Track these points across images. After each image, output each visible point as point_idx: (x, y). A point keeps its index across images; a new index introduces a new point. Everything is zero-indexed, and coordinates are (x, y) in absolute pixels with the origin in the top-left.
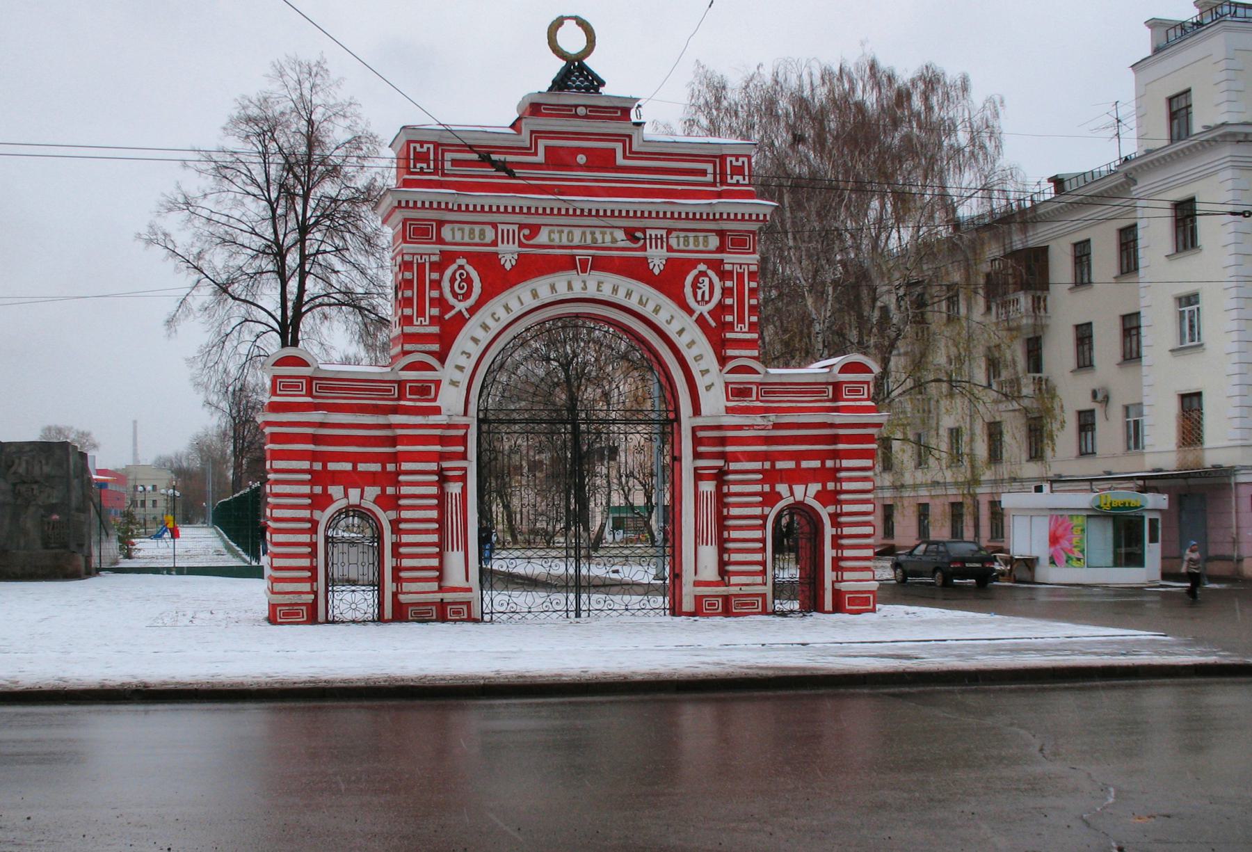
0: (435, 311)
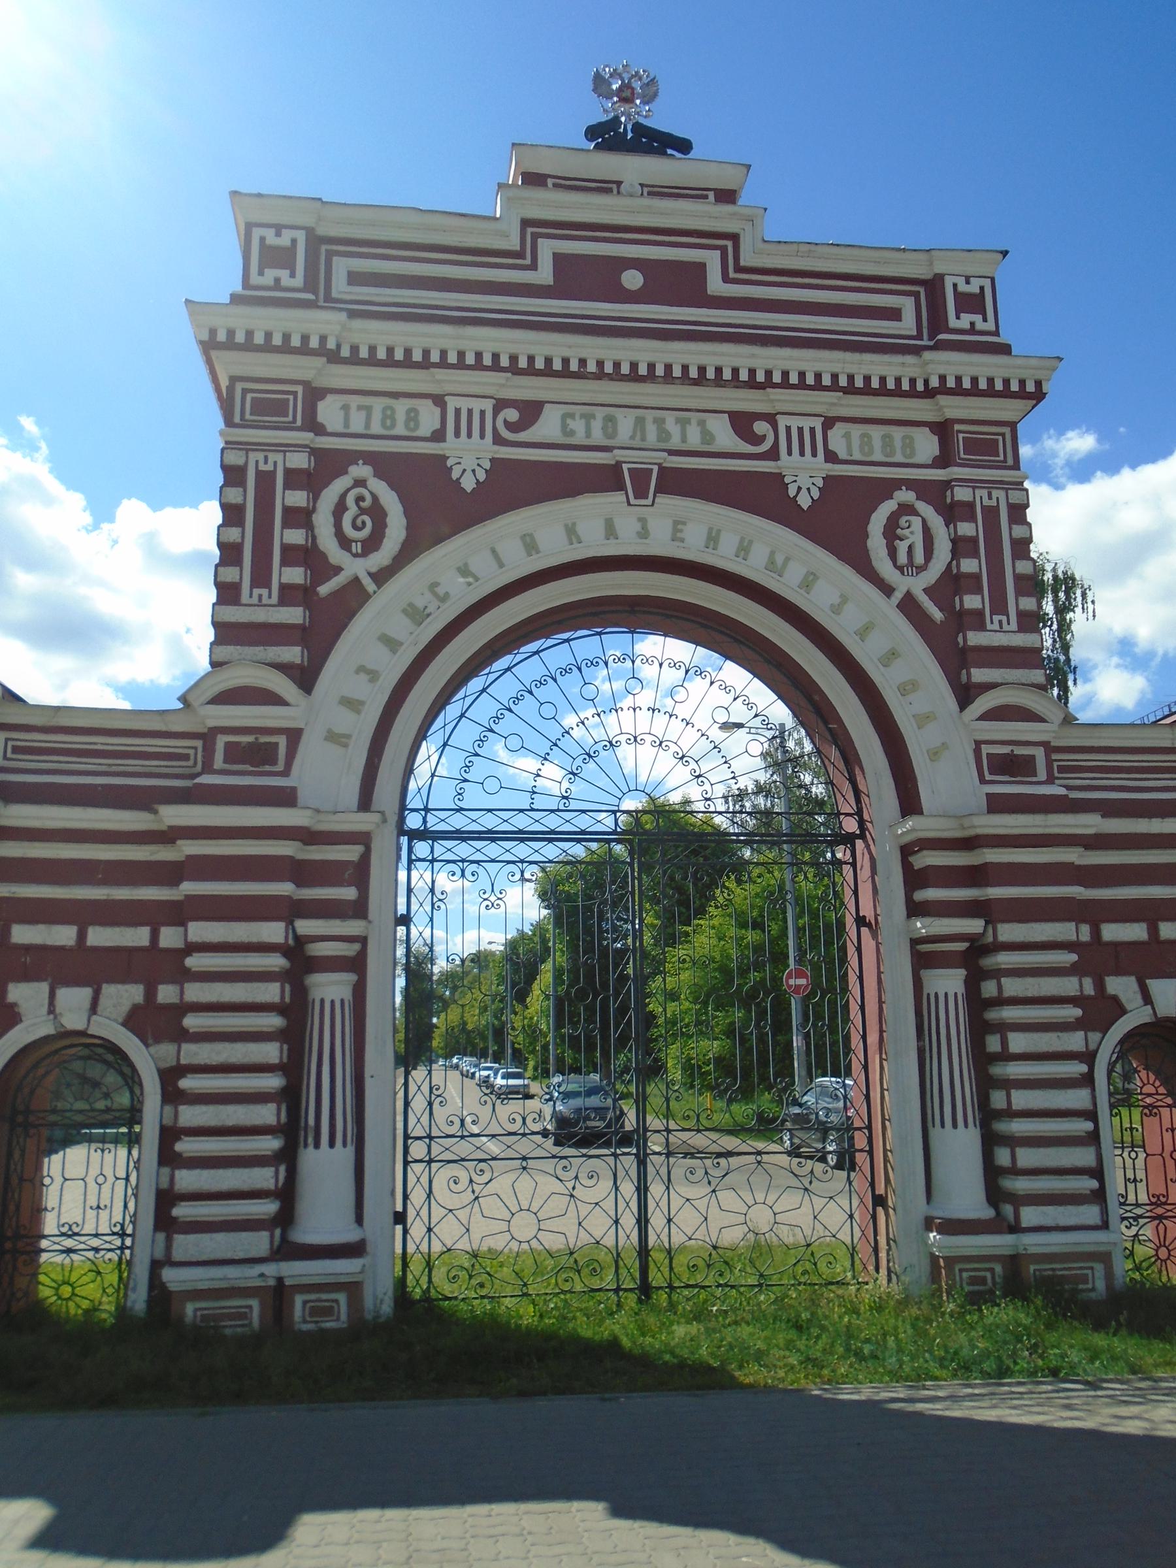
0: (295, 575)
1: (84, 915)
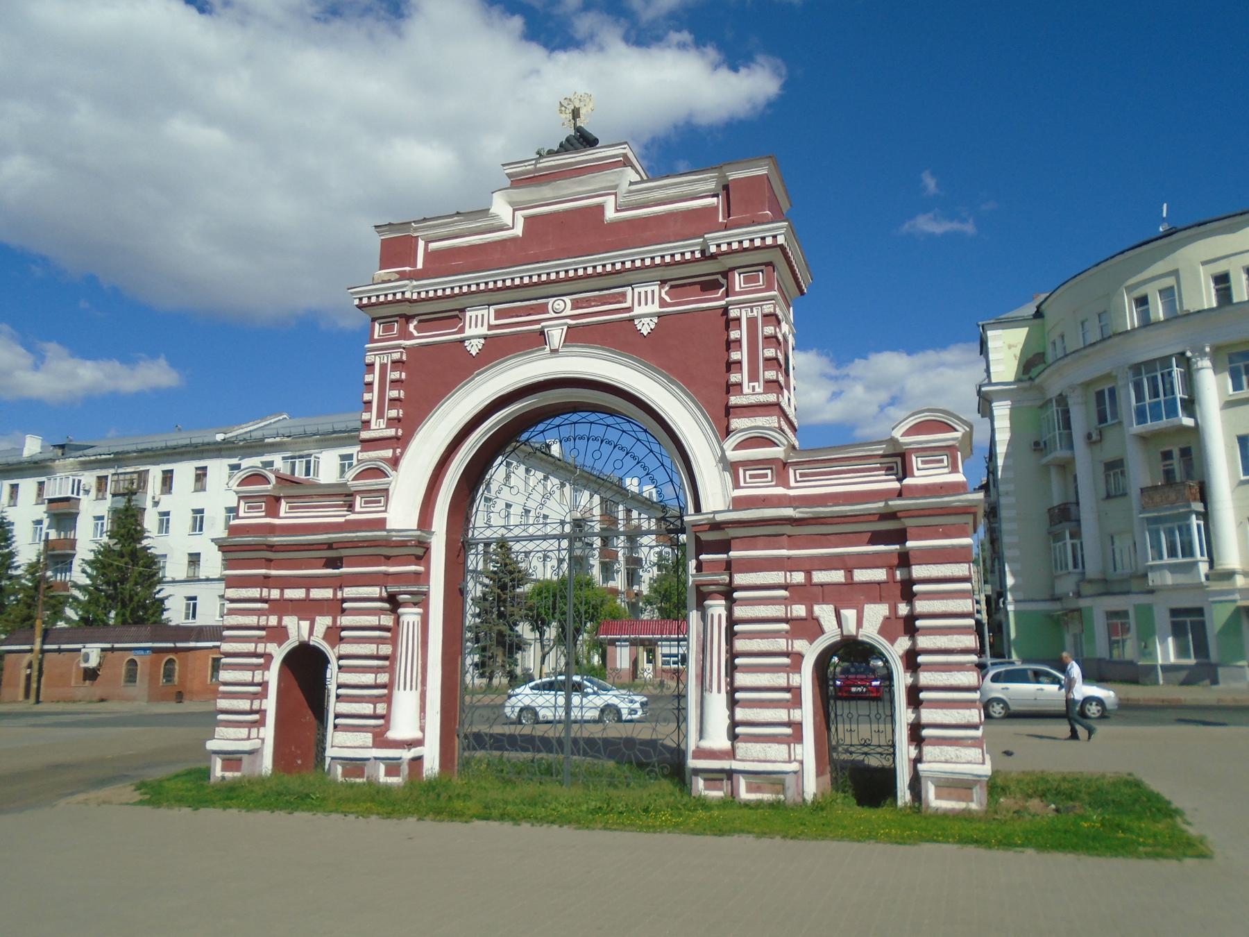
1: (309, 582)
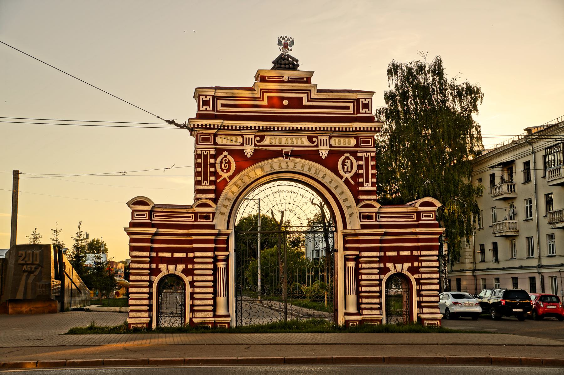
0: (213, 178)
1: (173, 250)
